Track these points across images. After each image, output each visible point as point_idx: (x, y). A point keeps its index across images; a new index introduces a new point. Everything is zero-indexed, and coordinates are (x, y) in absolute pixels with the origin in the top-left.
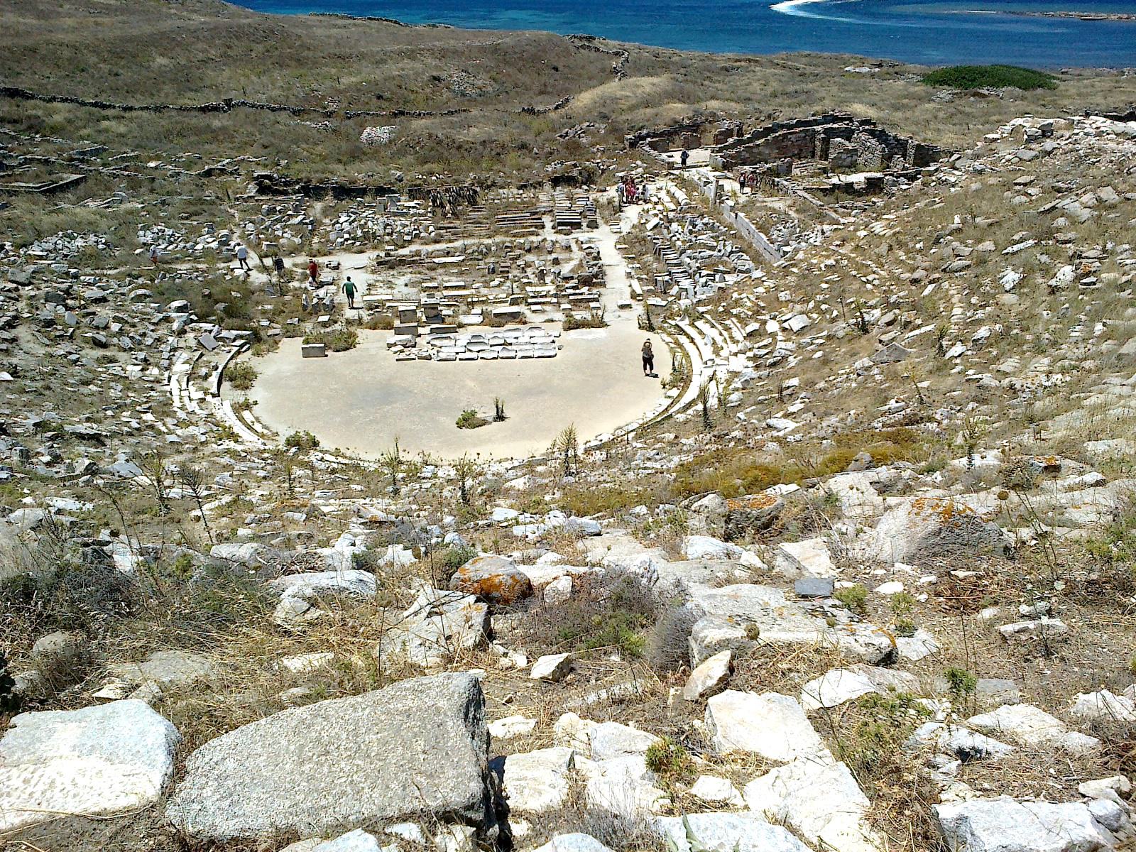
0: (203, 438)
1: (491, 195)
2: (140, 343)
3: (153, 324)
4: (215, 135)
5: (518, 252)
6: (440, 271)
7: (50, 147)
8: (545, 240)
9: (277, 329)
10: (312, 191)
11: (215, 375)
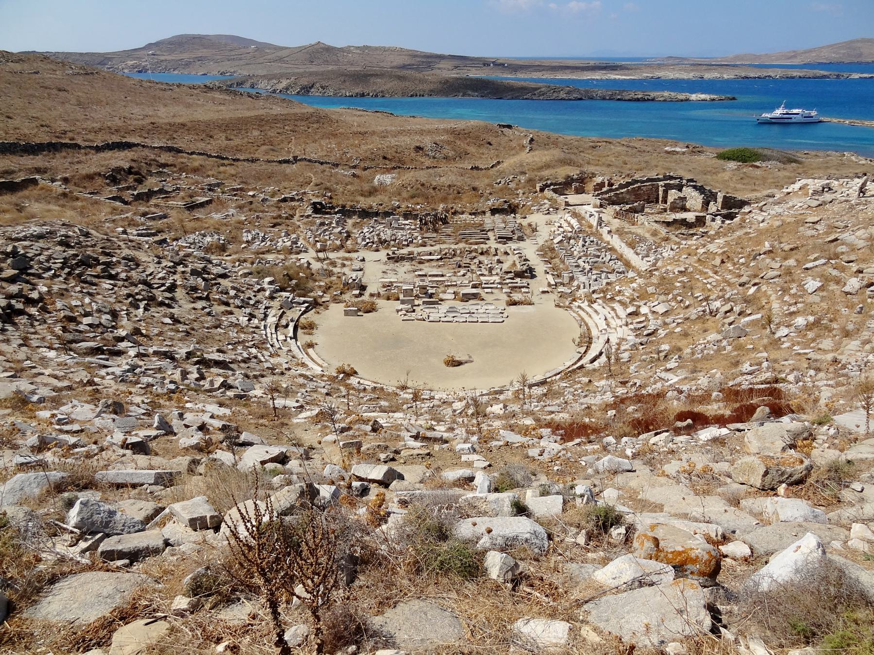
0: (286, 366)
1: (456, 218)
2: (248, 304)
4: (286, 177)
5: (474, 254)
6: (427, 264)
7: (190, 181)
8: (490, 247)
9: (327, 297)
10: (347, 213)
11: (292, 325)
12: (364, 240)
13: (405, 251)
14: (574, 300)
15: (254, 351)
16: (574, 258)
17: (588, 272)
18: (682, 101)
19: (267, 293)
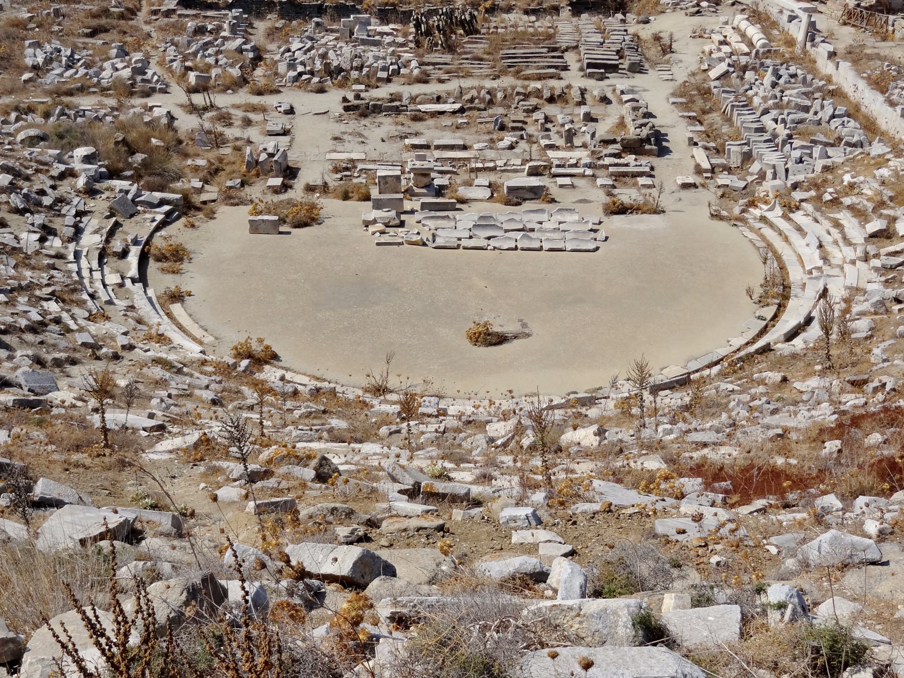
0: (124, 341)
1: (495, 20)
2: (39, 204)
3: (52, 177)
5: (533, 101)
6: (431, 122)
8: (569, 87)
9: (211, 193)
12: (291, 66)
13: (382, 93)
14: (752, 204)
15: (53, 307)
16: (752, 111)
17: (784, 143)
19: (81, 182)
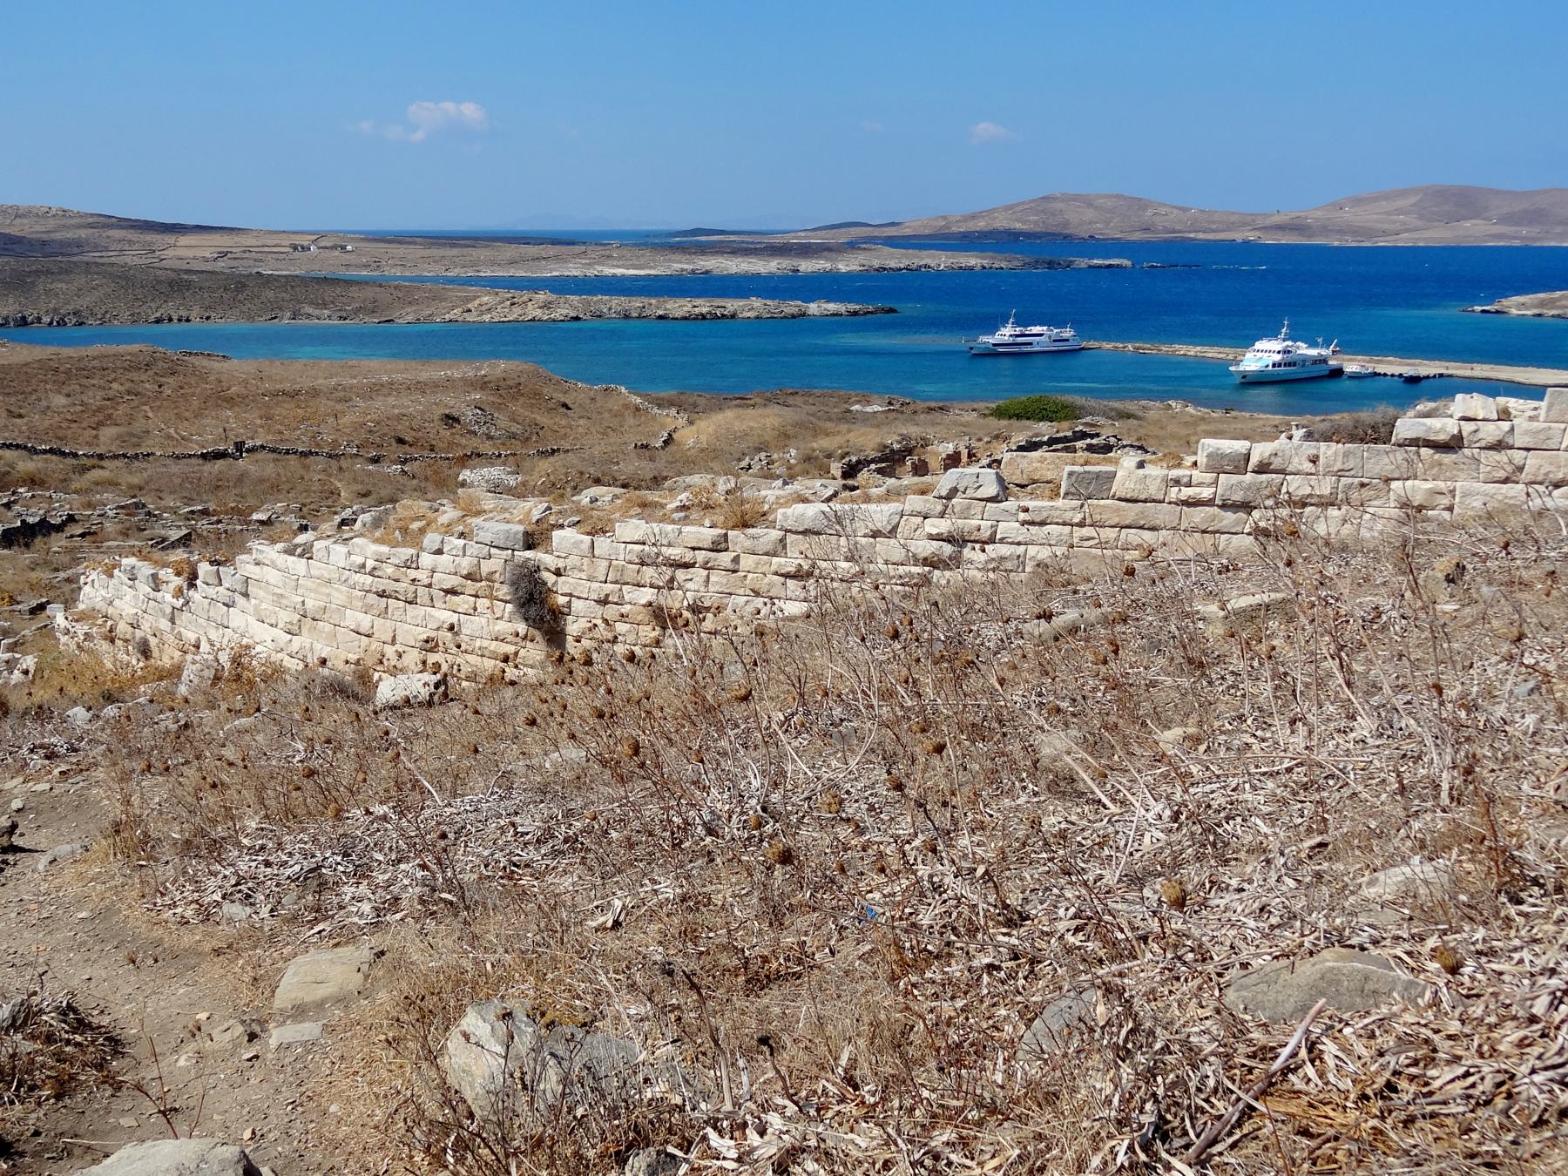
18: (793, 317)
